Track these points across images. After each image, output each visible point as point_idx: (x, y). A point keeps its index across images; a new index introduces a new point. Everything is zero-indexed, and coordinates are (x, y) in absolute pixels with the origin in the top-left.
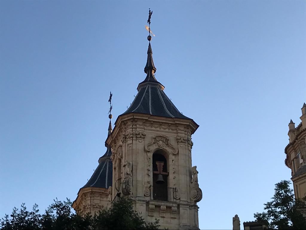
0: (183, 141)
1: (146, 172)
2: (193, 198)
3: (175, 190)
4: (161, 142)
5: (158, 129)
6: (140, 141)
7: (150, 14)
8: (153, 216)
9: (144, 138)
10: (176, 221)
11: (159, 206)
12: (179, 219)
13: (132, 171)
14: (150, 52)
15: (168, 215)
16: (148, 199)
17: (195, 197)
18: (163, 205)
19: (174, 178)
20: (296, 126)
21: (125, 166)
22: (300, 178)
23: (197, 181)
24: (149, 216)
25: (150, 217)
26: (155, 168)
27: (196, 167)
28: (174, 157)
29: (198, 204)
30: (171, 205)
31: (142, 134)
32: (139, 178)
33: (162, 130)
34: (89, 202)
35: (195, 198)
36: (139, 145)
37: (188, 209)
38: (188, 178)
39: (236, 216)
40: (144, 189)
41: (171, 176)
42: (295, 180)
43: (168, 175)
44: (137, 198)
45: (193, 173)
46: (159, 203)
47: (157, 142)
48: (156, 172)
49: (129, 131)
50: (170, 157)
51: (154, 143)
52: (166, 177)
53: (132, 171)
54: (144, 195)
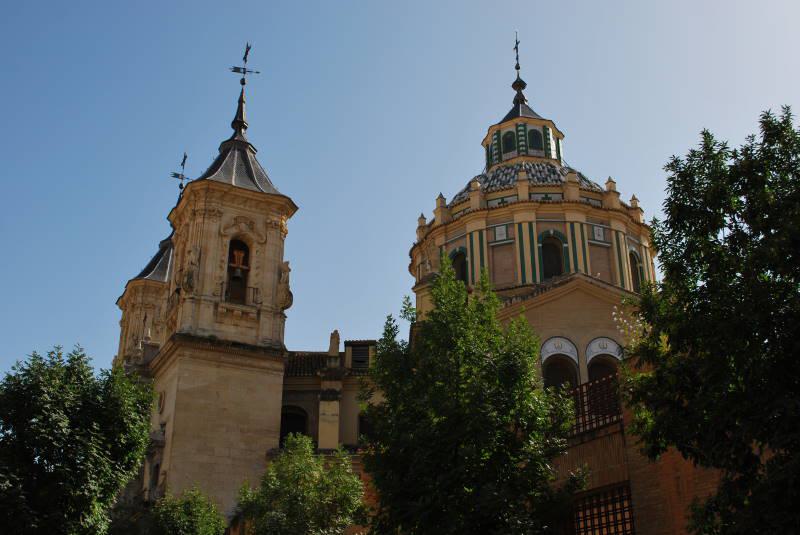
3: (256, 290)
4: (243, 224)
5: (242, 206)
7: (248, 49)
10: (254, 332)
11: (232, 311)
12: (258, 329)
13: (199, 260)
14: (241, 101)
15: (243, 323)
16: (217, 299)
18: (238, 309)
20: (428, 222)
21: (189, 252)
23: (287, 282)
26: (232, 258)
27: (287, 263)
28: (259, 247)
29: (286, 312)
30: (248, 309)
31: (219, 211)
32: (209, 270)
33: (247, 208)
34: (139, 299)
36: (213, 226)
38: (276, 277)
39: (336, 332)
41: (253, 273)
43: (248, 271)
44: (203, 298)
45: (282, 271)
48: (232, 265)
49: (201, 205)
52: (246, 272)
53: (199, 260)
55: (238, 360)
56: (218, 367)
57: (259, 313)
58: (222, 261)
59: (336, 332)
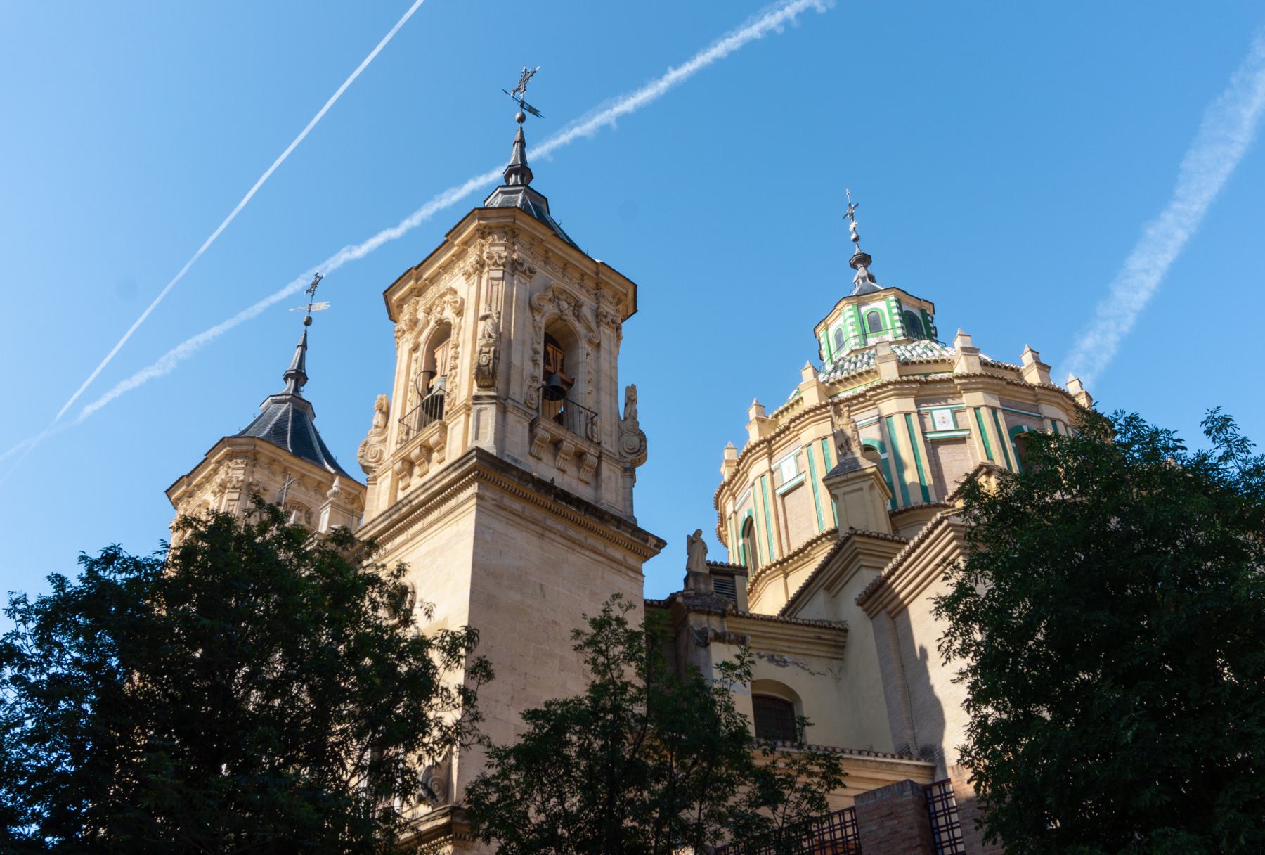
0: (610, 323)
1: (531, 353)
4: (565, 305)
6: (521, 279)
8: (540, 459)
9: (531, 277)
12: (597, 487)
19: (589, 393)
22: (848, 480)
24: (533, 456)
35: (632, 454)
37: (619, 472)
40: (525, 388)
42: (834, 484)
46: (561, 432)
47: (557, 300)
48: (548, 367)
51: (550, 300)
54: (525, 403)
56: (542, 536)
57: (599, 458)
58: (536, 352)
59: (699, 532)
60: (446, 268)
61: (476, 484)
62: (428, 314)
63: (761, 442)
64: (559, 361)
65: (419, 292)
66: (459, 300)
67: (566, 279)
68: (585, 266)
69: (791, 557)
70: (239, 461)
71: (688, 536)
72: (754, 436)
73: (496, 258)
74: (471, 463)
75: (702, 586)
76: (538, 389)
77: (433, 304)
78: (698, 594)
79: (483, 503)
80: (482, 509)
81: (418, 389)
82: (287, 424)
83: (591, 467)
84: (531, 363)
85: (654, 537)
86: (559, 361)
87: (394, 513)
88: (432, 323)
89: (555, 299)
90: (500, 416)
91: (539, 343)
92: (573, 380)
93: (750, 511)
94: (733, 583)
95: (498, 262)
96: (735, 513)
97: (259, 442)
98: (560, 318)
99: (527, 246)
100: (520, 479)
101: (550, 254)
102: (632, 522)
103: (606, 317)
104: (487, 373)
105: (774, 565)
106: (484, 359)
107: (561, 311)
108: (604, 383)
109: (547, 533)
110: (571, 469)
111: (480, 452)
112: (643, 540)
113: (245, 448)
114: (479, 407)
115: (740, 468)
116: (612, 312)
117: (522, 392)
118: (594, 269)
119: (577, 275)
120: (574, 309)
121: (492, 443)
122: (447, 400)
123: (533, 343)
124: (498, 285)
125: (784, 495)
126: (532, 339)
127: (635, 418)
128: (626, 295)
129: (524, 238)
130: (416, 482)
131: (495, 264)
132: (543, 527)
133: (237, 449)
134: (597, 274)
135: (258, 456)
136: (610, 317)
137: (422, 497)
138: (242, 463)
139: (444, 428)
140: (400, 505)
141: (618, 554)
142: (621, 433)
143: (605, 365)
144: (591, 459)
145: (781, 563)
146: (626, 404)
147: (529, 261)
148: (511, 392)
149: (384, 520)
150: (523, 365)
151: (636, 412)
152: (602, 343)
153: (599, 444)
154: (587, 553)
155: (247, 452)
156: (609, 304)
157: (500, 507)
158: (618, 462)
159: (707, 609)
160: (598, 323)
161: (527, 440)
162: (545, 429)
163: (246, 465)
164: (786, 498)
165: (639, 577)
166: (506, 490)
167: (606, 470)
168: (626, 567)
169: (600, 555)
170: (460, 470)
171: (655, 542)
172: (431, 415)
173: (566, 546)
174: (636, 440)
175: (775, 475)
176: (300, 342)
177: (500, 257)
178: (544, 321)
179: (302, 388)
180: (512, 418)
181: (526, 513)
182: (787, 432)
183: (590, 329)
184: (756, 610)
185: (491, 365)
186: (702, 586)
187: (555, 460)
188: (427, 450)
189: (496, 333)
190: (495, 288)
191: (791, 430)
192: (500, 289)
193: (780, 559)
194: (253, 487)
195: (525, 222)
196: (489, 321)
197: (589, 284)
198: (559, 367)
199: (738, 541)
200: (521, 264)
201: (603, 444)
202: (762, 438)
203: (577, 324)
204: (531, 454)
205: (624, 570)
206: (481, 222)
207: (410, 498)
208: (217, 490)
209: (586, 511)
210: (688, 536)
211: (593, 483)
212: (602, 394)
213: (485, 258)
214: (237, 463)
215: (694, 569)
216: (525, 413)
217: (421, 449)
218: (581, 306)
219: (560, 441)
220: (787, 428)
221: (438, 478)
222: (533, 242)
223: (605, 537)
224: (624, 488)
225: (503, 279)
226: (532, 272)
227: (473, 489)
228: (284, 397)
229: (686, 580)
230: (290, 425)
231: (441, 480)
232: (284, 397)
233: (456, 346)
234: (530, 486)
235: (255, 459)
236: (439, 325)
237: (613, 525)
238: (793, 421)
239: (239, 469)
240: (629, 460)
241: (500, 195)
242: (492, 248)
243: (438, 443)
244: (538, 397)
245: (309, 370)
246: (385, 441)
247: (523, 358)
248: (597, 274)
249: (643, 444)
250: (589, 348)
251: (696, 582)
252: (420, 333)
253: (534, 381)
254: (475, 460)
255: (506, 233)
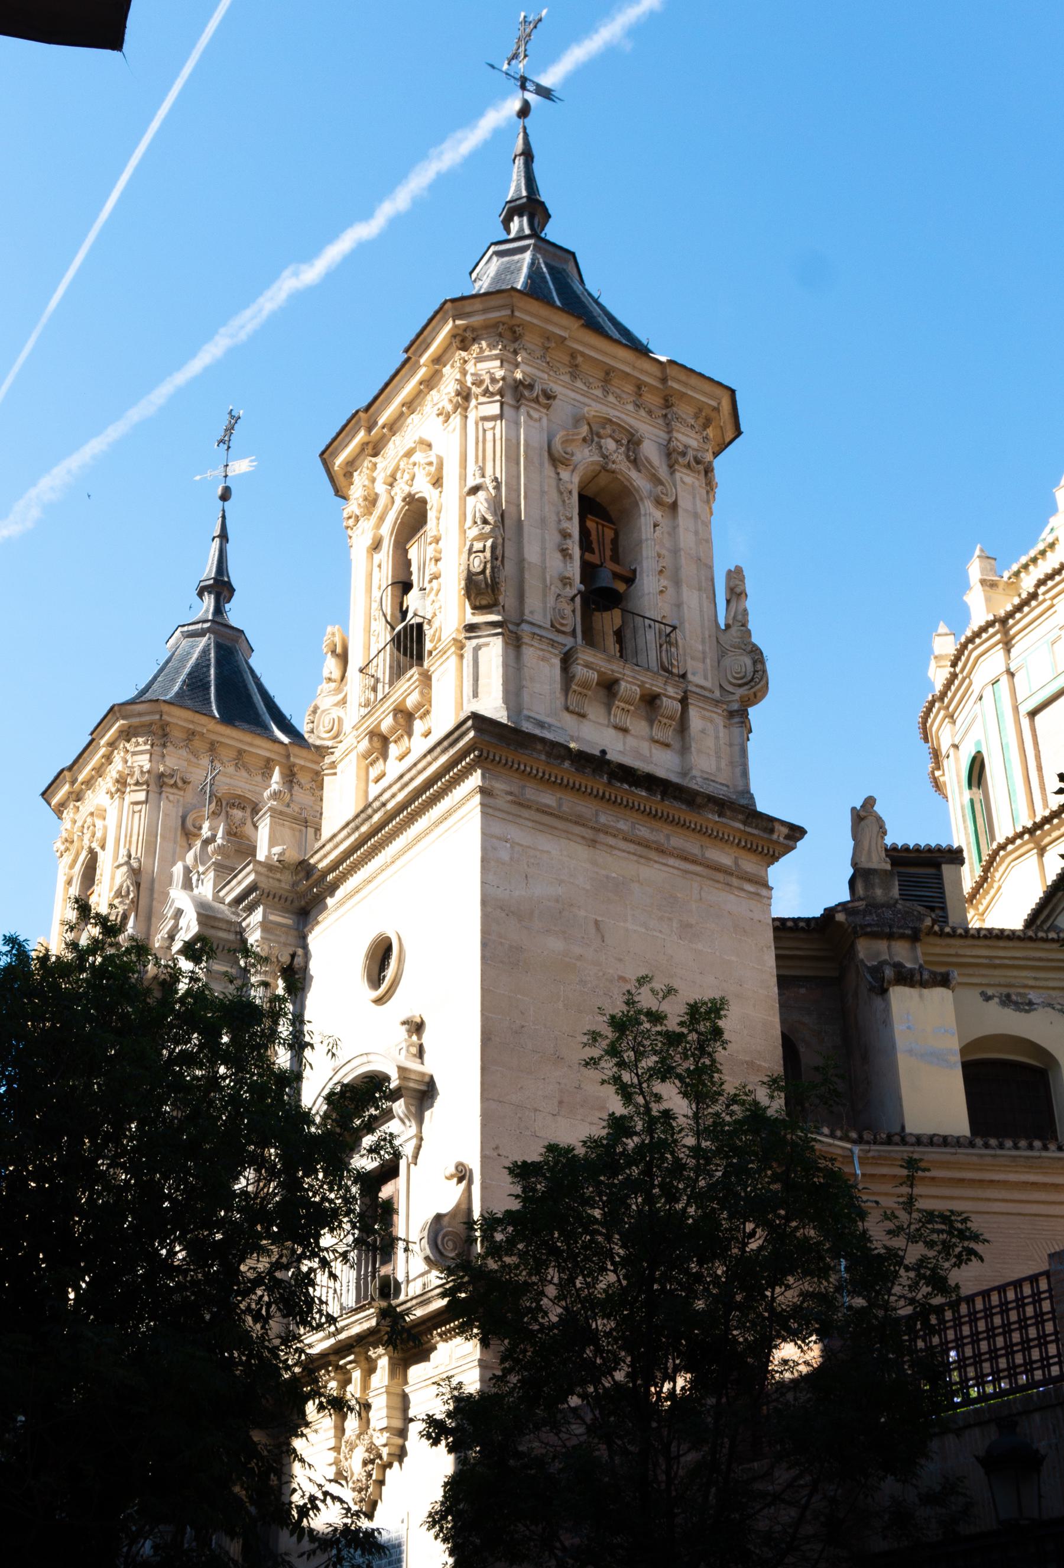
0: (693, 463)
1: (557, 538)
2: (734, 685)
3: (669, 635)
4: (610, 445)
6: (532, 412)
8: (583, 716)
9: (548, 407)
12: (684, 750)
17: (740, 682)
19: (661, 592)
24: (572, 712)
25: (575, 717)
35: (740, 686)
37: (720, 721)
40: (551, 601)
46: (614, 667)
47: (596, 439)
48: (588, 556)
50: (643, 512)
51: (584, 440)
54: (552, 626)
55: (643, 832)
56: (593, 843)
57: (684, 701)
58: (565, 535)
59: (870, 802)
60: (411, 405)
61: (479, 771)
62: (391, 485)
63: (990, 624)
64: (608, 541)
65: (375, 448)
66: (434, 460)
67: (611, 399)
68: (642, 371)
69: (1047, 820)
70: (141, 740)
71: (853, 809)
72: (979, 617)
73: (487, 381)
74: (466, 739)
75: (879, 892)
76: (573, 599)
77: (397, 468)
78: (873, 906)
79: (490, 801)
80: (490, 811)
81: (385, 616)
82: (209, 670)
83: (671, 718)
84: (558, 556)
85: (783, 823)
86: (608, 541)
87: (362, 824)
88: (399, 503)
89: (593, 438)
90: (512, 652)
91: (570, 519)
92: (634, 571)
93: (978, 743)
94: (939, 877)
95: (491, 389)
96: (956, 746)
97: (165, 708)
98: (604, 468)
99: (539, 353)
100: (549, 755)
101: (580, 359)
102: (743, 802)
103: (684, 454)
104: (483, 586)
105: (1020, 835)
106: (477, 562)
107: (605, 457)
108: (688, 570)
109: (602, 837)
110: (639, 726)
111: (478, 720)
112: (765, 830)
113: (146, 719)
114: (474, 642)
115: (958, 669)
116: (694, 444)
117: (545, 609)
118: (659, 374)
119: (629, 388)
120: (628, 449)
121: (501, 701)
122: (428, 632)
123: (560, 521)
124: (494, 428)
125: (1033, 714)
126: (558, 514)
127: (744, 625)
128: (717, 410)
129: (531, 340)
130: (393, 767)
131: (486, 392)
132: (593, 828)
133: (135, 721)
134: (664, 380)
135: (168, 729)
136: (691, 453)
137: (400, 797)
138: (145, 743)
139: (426, 679)
140: (370, 811)
141: (724, 857)
142: (722, 653)
143: (686, 539)
144: (670, 705)
145: (1031, 831)
146: (728, 602)
147: (545, 379)
148: (527, 612)
149: (349, 835)
150: (544, 561)
151: (745, 612)
152: (680, 503)
153: (684, 676)
154: (671, 861)
155: (151, 725)
156: (688, 431)
157: (520, 805)
158: (717, 703)
159: (887, 930)
160: (671, 466)
161: (558, 686)
162: (588, 666)
163: (152, 745)
164: (1037, 718)
165: (764, 892)
166: (527, 775)
167: (696, 719)
168: (738, 877)
169: (694, 862)
170: (452, 751)
171: (785, 831)
172: (412, 657)
173: (634, 854)
174: (748, 662)
175: (1016, 679)
176: (217, 532)
177: (494, 380)
178: (576, 479)
179: (227, 606)
180: (530, 654)
181: (565, 808)
182: (1034, 603)
183: (657, 481)
184: (974, 924)
185: (488, 571)
186: (879, 892)
187: (610, 714)
188: (406, 717)
189: (495, 514)
190: (489, 435)
191: (1041, 598)
192: (498, 436)
193: (1029, 825)
194: (166, 780)
195: (531, 313)
196: (481, 494)
197: (653, 400)
198: (608, 553)
199: (961, 793)
200: (531, 387)
201: (690, 677)
202: (991, 618)
203: (634, 474)
204: (567, 709)
205: (735, 882)
206: (458, 322)
207: (383, 798)
208: (113, 790)
209: (664, 794)
210: (853, 809)
211: (676, 745)
212: (685, 589)
213: (469, 384)
214: (138, 744)
215: (865, 864)
216: (553, 643)
217: (395, 716)
218: (639, 443)
219: (616, 682)
220: (1034, 596)
221: (420, 766)
222: (547, 345)
223: (701, 832)
224: (731, 745)
225: (501, 417)
226: (549, 396)
227: (475, 779)
228: (199, 626)
229: (852, 883)
230: (212, 671)
231: (424, 769)
232: (199, 626)
233: (437, 540)
234: (567, 764)
235: (165, 735)
236: (408, 504)
237: (713, 812)
238: (1041, 583)
239: (141, 752)
240: (736, 697)
241: (495, 258)
242: (480, 366)
243: (420, 706)
244: (574, 611)
245: (235, 576)
246: (344, 702)
247: (543, 548)
248: (664, 380)
249: (759, 666)
250: (657, 514)
251: (868, 885)
252: (382, 519)
253: (565, 585)
254: (472, 734)
255: (500, 335)
